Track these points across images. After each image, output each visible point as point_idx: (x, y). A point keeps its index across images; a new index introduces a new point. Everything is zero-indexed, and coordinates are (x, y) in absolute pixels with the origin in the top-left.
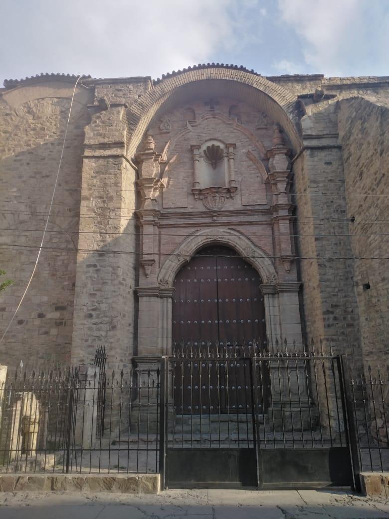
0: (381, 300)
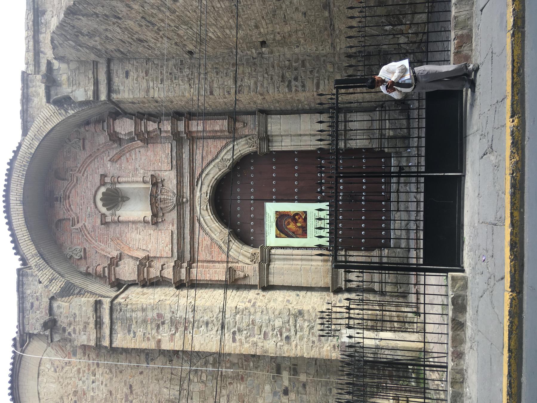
0: (278, 30)
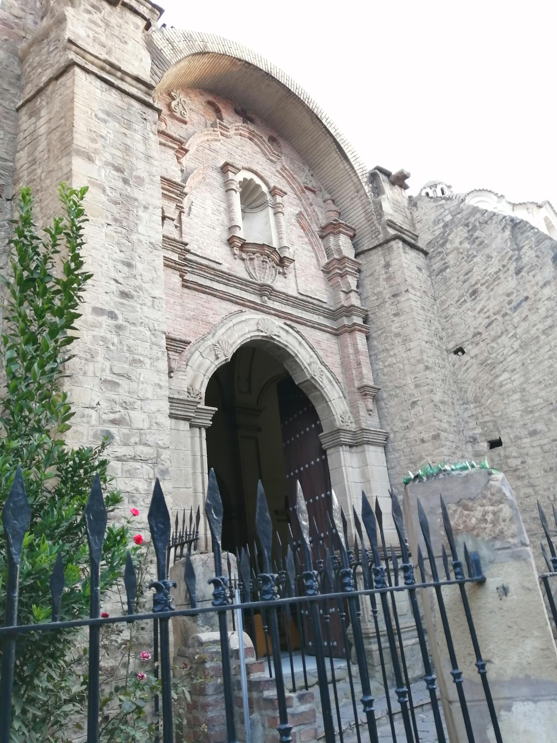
0: (530, 461)
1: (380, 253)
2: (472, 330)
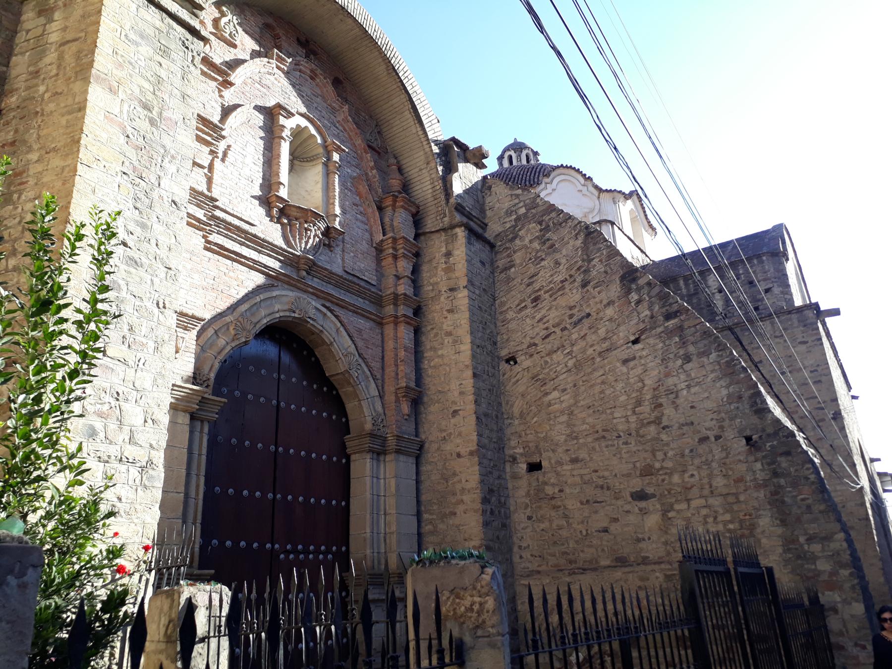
0: (567, 490)
1: (443, 238)
2: (528, 339)
